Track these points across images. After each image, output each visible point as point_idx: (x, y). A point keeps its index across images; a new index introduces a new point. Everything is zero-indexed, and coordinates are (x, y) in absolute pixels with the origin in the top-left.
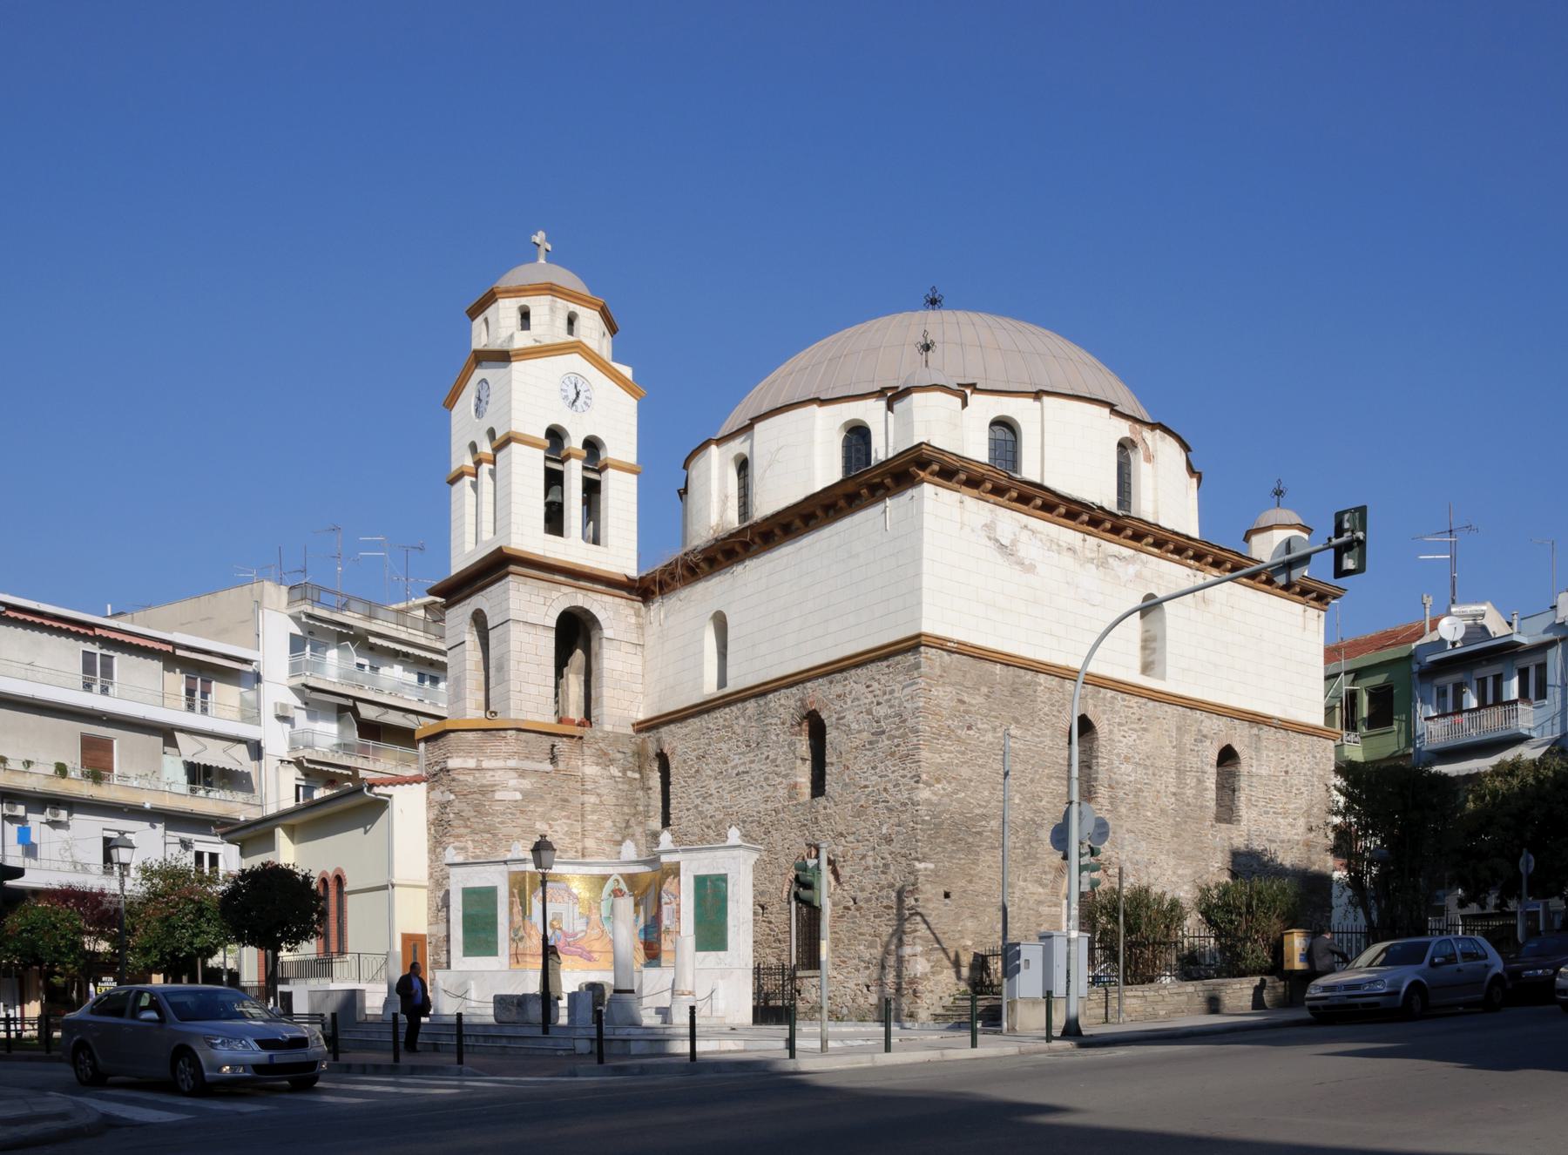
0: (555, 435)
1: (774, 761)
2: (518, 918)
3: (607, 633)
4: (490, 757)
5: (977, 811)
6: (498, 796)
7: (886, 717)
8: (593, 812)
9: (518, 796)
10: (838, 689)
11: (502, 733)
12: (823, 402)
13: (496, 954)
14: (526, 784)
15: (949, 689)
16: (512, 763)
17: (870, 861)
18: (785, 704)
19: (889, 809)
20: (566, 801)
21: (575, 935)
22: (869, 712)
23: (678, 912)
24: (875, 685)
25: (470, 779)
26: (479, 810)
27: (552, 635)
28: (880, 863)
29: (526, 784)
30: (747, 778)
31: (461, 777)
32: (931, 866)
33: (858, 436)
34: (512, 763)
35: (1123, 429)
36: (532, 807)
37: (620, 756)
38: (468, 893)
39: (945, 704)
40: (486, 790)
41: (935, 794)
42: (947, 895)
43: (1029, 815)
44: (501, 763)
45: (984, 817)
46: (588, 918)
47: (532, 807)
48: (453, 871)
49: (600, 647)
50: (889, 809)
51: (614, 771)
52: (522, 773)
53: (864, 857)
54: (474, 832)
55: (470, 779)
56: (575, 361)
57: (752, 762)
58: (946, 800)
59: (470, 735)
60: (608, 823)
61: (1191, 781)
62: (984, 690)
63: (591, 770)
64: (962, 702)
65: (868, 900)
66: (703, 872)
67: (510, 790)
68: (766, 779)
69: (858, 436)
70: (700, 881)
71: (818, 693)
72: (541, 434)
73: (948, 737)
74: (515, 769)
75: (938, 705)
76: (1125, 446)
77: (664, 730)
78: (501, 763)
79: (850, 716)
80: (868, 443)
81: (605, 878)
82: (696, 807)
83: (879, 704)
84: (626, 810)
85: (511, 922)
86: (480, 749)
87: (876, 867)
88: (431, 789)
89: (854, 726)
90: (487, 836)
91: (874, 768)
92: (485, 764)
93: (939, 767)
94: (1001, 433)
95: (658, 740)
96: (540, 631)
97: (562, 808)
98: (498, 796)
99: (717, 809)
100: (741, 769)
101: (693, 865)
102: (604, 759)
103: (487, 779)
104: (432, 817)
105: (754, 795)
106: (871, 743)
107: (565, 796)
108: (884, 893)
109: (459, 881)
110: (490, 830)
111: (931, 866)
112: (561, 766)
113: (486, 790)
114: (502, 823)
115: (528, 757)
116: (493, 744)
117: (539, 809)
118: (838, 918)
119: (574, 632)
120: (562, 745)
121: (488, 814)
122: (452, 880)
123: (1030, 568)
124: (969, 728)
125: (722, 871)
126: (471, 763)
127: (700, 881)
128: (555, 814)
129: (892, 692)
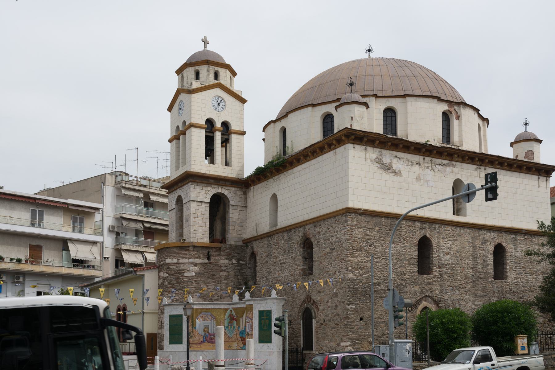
0: (210, 122)
1: (294, 259)
3: (232, 203)
4: (182, 258)
5: (375, 282)
6: (186, 274)
7: (336, 242)
8: (225, 279)
9: (194, 274)
10: (318, 229)
12: (313, 105)
14: (197, 269)
15: (360, 230)
17: (329, 304)
18: (297, 237)
19: (336, 281)
20: (214, 275)
22: (329, 240)
23: (252, 326)
24: (331, 229)
25: (175, 267)
26: (178, 280)
27: (208, 205)
28: (334, 305)
29: (197, 269)
31: (171, 267)
32: (354, 307)
33: (328, 119)
35: (445, 107)
36: (199, 279)
37: (236, 255)
38: (171, 317)
39: (359, 236)
40: (181, 272)
41: (355, 275)
42: (361, 319)
43: (399, 282)
44: (187, 261)
45: (378, 284)
48: (166, 308)
49: (229, 209)
50: (336, 281)
51: (234, 261)
52: (196, 264)
53: (327, 302)
55: (175, 267)
56: (218, 92)
57: (286, 259)
58: (360, 277)
59: (175, 249)
60: (232, 284)
61: (480, 261)
62: (377, 229)
63: (224, 261)
64: (367, 235)
65: (330, 321)
66: (262, 309)
67: (192, 271)
68: (292, 266)
69: (328, 119)
70: (261, 313)
71: (311, 230)
72: (203, 123)
73: (361, 251)
75: (355, 237)
76: (446, 117)
77: (254, 243)
78: (187, 261)
79: (322, 241)
80: (332, 121)
81: (226, 310)
82: (266, 277)
83: (332, 236)
84: (239, 277)
86: (179, 255)
87: (332, 307)
88: (159, 272)
89: (323, 246)
90: (180, 291)
91: (331, 264)
92: (181, 261)
93: (357, 263)
94: (389, 114)
96: (203, 204)
97: (212, 278)
98: (186, 274)
99: (274, 278)
100: (282, 262)
101: (259, 306)
102: (229, 257)
103: (182, 267)
104: (160, 283)
105: (286, 273)
106: (330, 253)
107: (214, 273)
108: (335, 318)
109: (169, 311)
111: (354, 307)
112: (212, 260)
113: (181, 272)
115: (198, 257)
118: (318, 328)
119: (218, 205)
121: (182, 282)
122: (165, 311)
123: (397, 173)
124: (370, 246)
125: (269, 309)
126: (175, 261)
127: (261, 313)
128: (209, 281)
129: (337, 231)
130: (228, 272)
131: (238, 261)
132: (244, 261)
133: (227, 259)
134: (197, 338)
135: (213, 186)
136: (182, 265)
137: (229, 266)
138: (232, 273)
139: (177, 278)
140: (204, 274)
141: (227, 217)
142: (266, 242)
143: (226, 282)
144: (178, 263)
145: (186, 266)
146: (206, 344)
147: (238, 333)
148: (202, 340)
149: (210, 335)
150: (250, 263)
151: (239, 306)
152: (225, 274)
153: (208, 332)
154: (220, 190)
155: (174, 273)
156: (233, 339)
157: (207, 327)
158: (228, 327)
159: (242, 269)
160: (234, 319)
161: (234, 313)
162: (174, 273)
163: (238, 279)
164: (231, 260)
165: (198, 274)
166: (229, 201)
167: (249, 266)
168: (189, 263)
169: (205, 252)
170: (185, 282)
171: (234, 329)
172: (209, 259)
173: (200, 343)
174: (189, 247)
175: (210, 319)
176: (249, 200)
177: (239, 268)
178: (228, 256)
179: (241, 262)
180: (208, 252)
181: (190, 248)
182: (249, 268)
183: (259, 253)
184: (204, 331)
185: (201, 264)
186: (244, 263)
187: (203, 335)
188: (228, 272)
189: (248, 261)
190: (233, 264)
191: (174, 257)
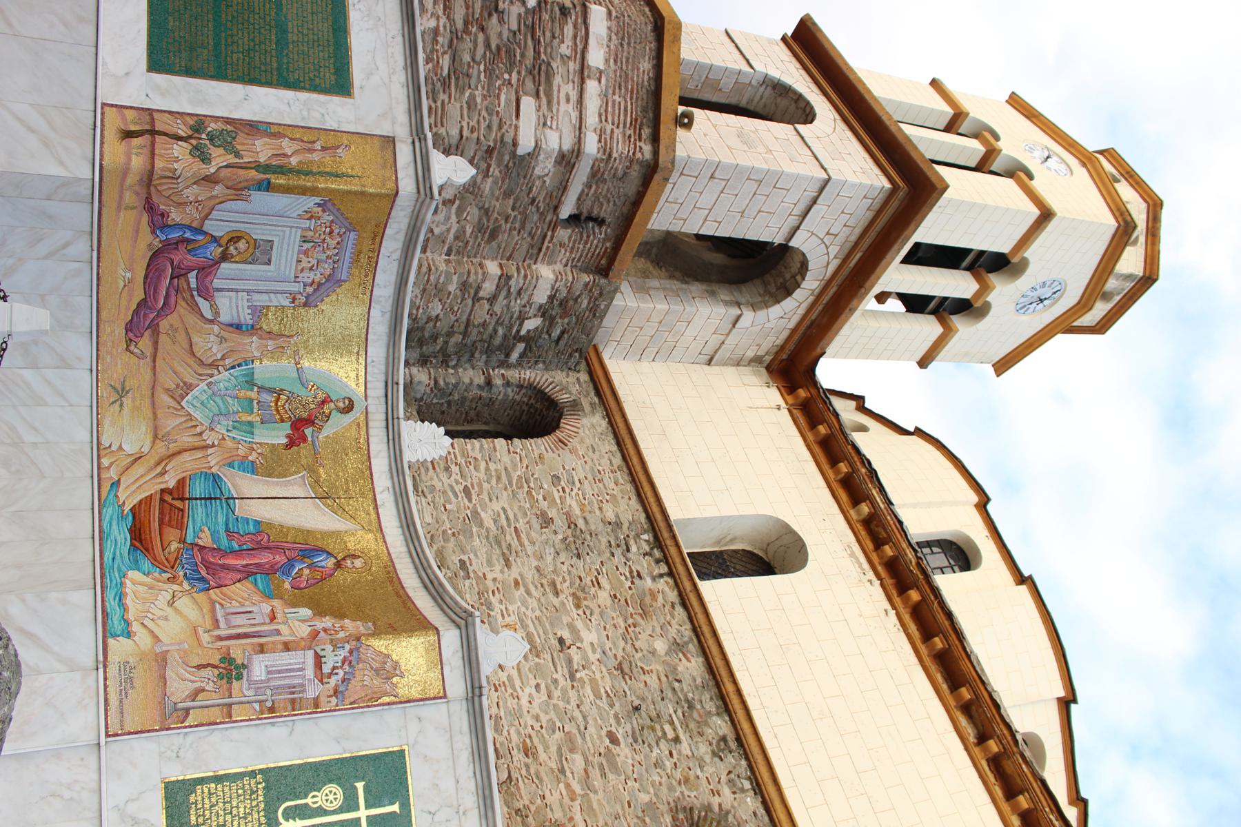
2: (262, 150)
3: (748, 316)
4: (604, 96)
6: (528, 103)
8: (464, 286)
11: (646, 132)
13: (158, 61)
14: (545, 167)
16: (591, 145)
20: (493, 235)
21: (206, 293)
23: (294, 705)
25: (565, 49)
26: (502, 56)
29: (545, 167)
30: (561, 675)
31: (569, 30)
34: (591, 145)
36: (495, 171)
37: (556, 333)
40: (540, 77)
44: (592, 119)
46: (253, 329)
47: (495, 171)
49: (727, 303)
51: (531, 324)
52: (568, 161)
54: (455, 37)
55: (565, 49)
59: (646, 65)
74: (577, 152)
78: (592, 119)
84: (458, 338)
85: (253, 128)
90: (445, 62)
92: (592, 86)
95: (575, 406)
97: (480, 228)
100: (576, 658)
102: (559, 305)
103: (564, 87)
107: (503, 237)
110: (456, 78)
112: (563, 234)
114: (471, 104)
115: (596, 175)
116: (628, 105)
117: (487, 186)
120: (599, 238)
121: (489, 72)
126: (596, 57)
128: (473, 213)
130: (492, 299)
131: (529, 339)
132: (522, 356)
133: (551, 298)
134: (192, 192)
135: (834, 264)
136: (571, 90)
137: (516, 306)
138: (481, 314)
139: (510, 53)
140: (507, 195)
141: (696, 288)
142: (626, 518)
143: (452, 288)
144: (583, 73)
145: (567, 111)
146: (147, 241)
147: (214, 460)
148: (176, 216)
149: (207, 270)
150: (508, 384)
151: (380, 465)
152: (489, 288)
153: (225, 257)
154: (810, 284)
155: (537, 42)
156: (170, 423)
157: (260, 252)
158: (251, 383)
159: (489, 352)
160: (299, 425)
161: (336, 425)
162: (537, 42)
163: (450, 334)
164: (543, 312)
165: (520, 165)
166: (754, 307)
167: (498, 382)
168: (580, 128)
169: (606, 211)
170: (492, 93)
171: (238, 425)
172: (574, 219)
173: (150, 207)
174: (655, 139)
175: (307, 277)
176: (731, 370)
177: (498, 341)
178: (563, 304)
179: (521, 347)
180: (600, 222)
181: (647, 148)
182: (489, 383)
183: (570, 460)
184: (235, 239)
185: (564, 187)
186: (515, 356)
187: (209, 226)
188: (492, 299)
189: (514, 375)
190: (522, 319)
191: (614, 57)
